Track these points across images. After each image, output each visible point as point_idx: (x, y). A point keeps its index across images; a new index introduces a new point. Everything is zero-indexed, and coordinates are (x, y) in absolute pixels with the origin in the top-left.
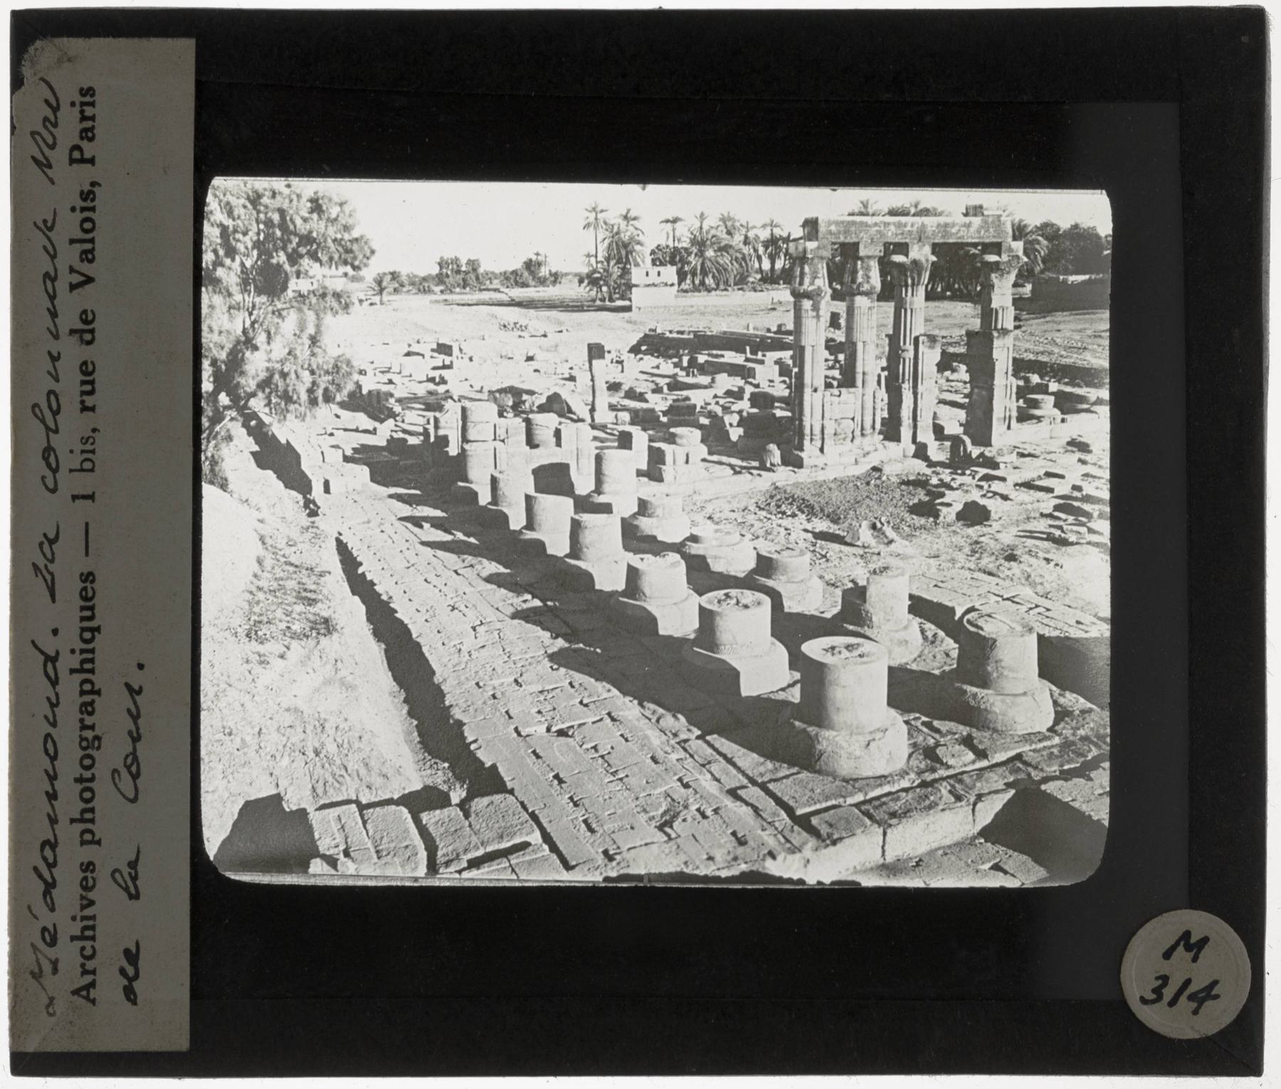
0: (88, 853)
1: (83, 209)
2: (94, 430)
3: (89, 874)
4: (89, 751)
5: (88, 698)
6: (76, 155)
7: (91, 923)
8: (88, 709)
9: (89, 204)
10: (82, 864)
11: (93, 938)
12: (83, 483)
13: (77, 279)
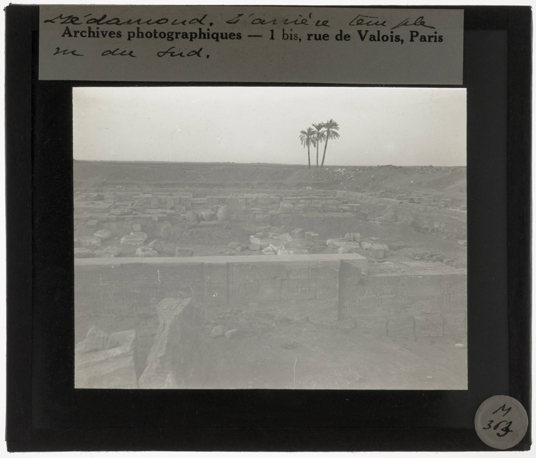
0: (125, 35)
1: (392, 36)
2: (300, 40)
3: (116, 35)
4: (167, 36)
5: (189, 36)
6: (415, 34)
7: (96, 35)
8: (185, 36)
9: (394, 39)
10: (120, 32)
11: (89, 36)
12: (278, 34)
13: (363, 33)
